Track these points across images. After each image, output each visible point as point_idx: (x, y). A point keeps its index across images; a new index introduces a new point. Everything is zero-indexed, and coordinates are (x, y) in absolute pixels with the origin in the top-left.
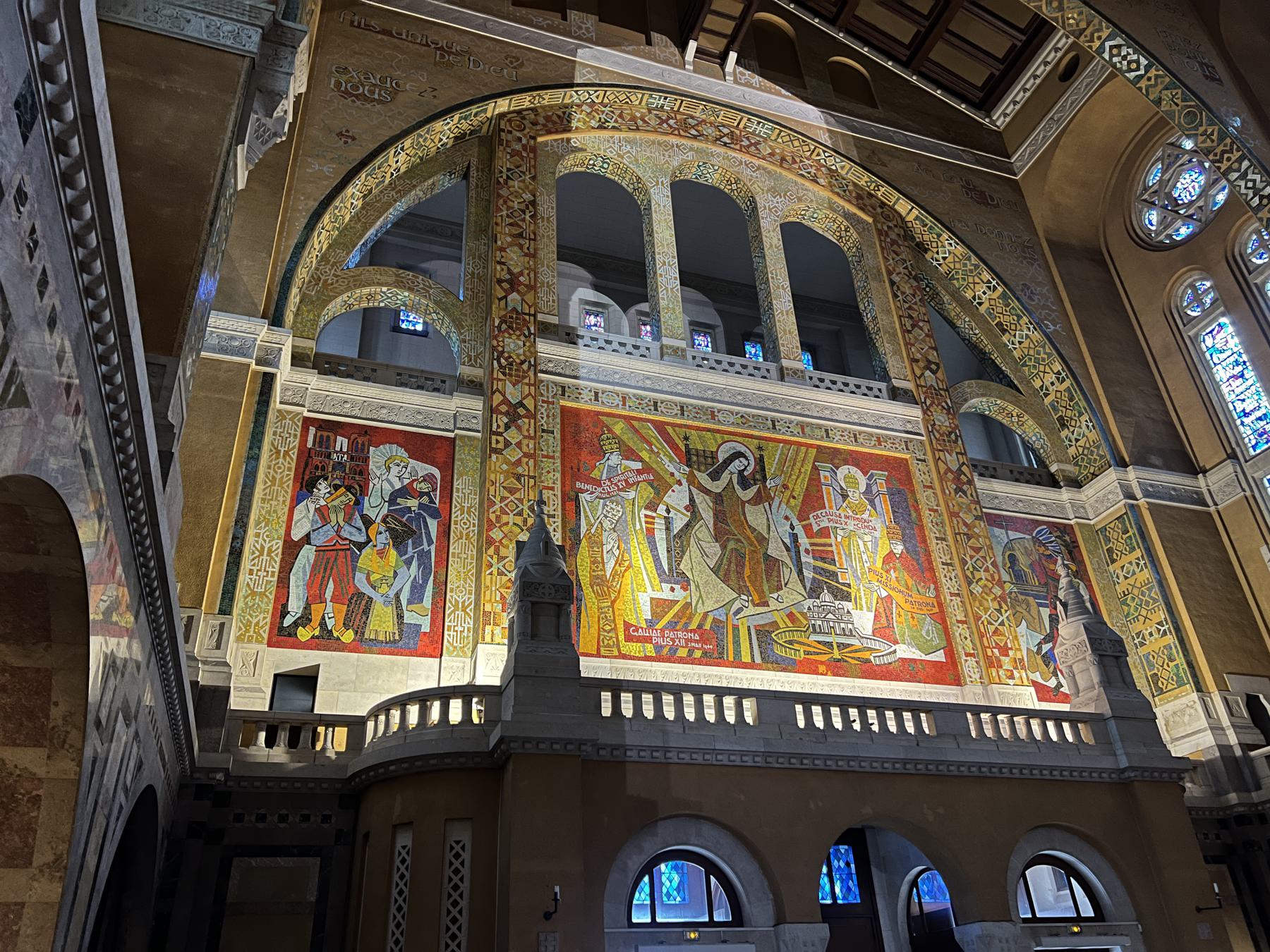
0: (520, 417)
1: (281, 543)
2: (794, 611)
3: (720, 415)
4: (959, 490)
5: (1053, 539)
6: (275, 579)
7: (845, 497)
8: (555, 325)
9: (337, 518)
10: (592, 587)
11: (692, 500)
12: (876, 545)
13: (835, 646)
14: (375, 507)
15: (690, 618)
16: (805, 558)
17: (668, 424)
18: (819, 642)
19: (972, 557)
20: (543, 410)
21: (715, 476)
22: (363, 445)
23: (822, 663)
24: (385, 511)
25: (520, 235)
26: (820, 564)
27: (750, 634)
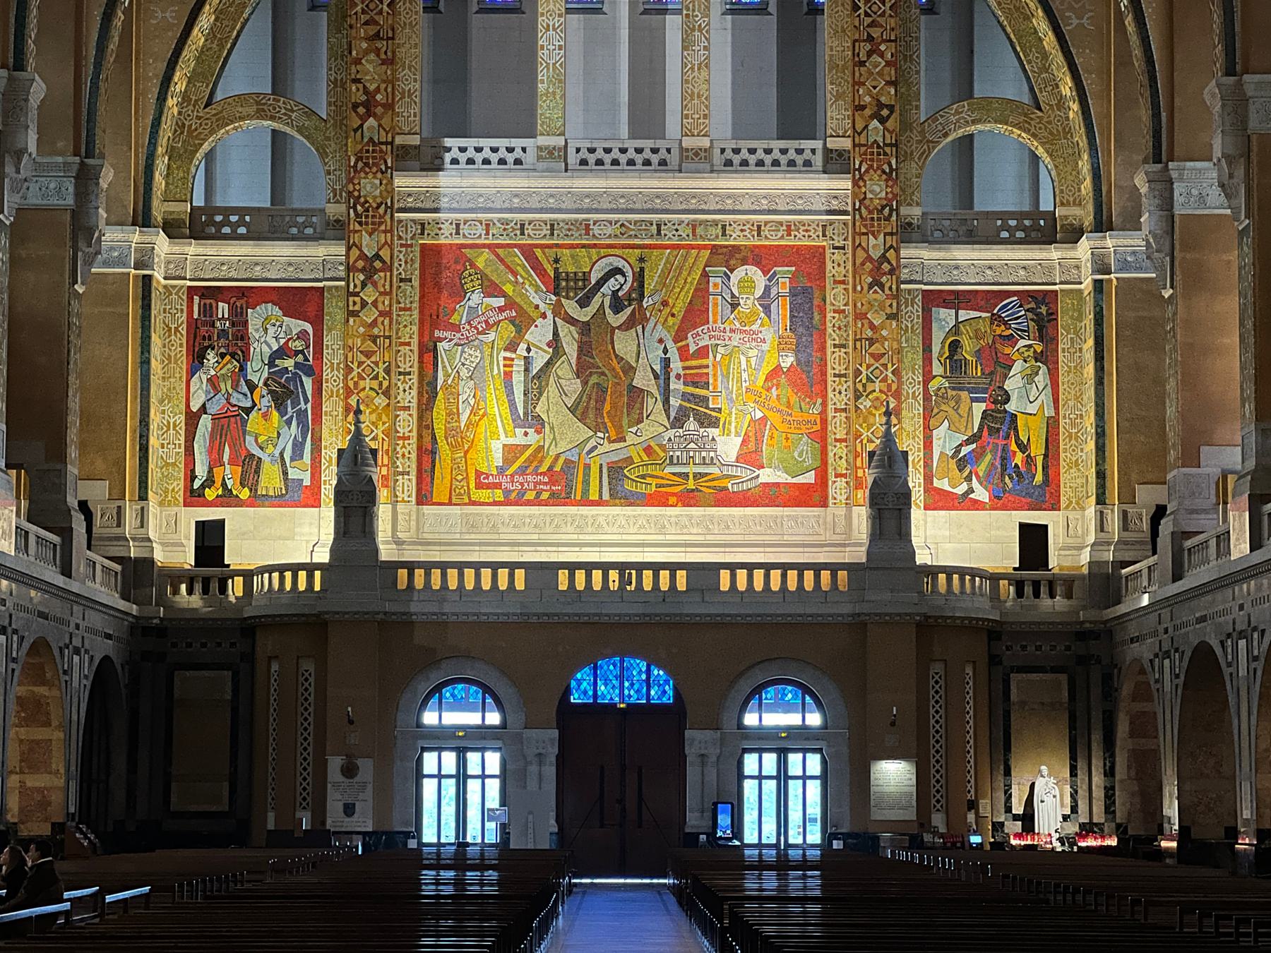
0: (376, 271)
1: (183, 418)
2: (652, 444)
3: (595, 228)
4: (877, 283)
5: (1023, 313)
6: (183, 449)
7: (734, 306)
8: (416, 147)
9: (225, 386)
10: (447, 440)
11: (556, 334)
12: (761, 359)
13: (691, 476)
14: (257, 372)
15: (541, 462)
16: (676, 385)
17: (537, 246)
18: (674, 474)
19: (868, 367)
20: (401, 256)
21: (583, 303)
22: (242, 308)
23: (673, 494)
24: (266, 375)
25: (377, 36)
26: (690, 389)
27: (601, 471)
